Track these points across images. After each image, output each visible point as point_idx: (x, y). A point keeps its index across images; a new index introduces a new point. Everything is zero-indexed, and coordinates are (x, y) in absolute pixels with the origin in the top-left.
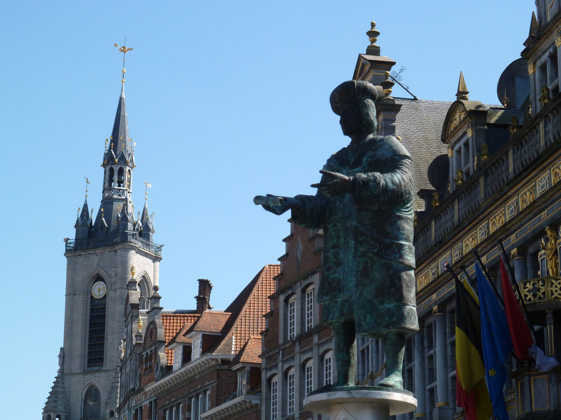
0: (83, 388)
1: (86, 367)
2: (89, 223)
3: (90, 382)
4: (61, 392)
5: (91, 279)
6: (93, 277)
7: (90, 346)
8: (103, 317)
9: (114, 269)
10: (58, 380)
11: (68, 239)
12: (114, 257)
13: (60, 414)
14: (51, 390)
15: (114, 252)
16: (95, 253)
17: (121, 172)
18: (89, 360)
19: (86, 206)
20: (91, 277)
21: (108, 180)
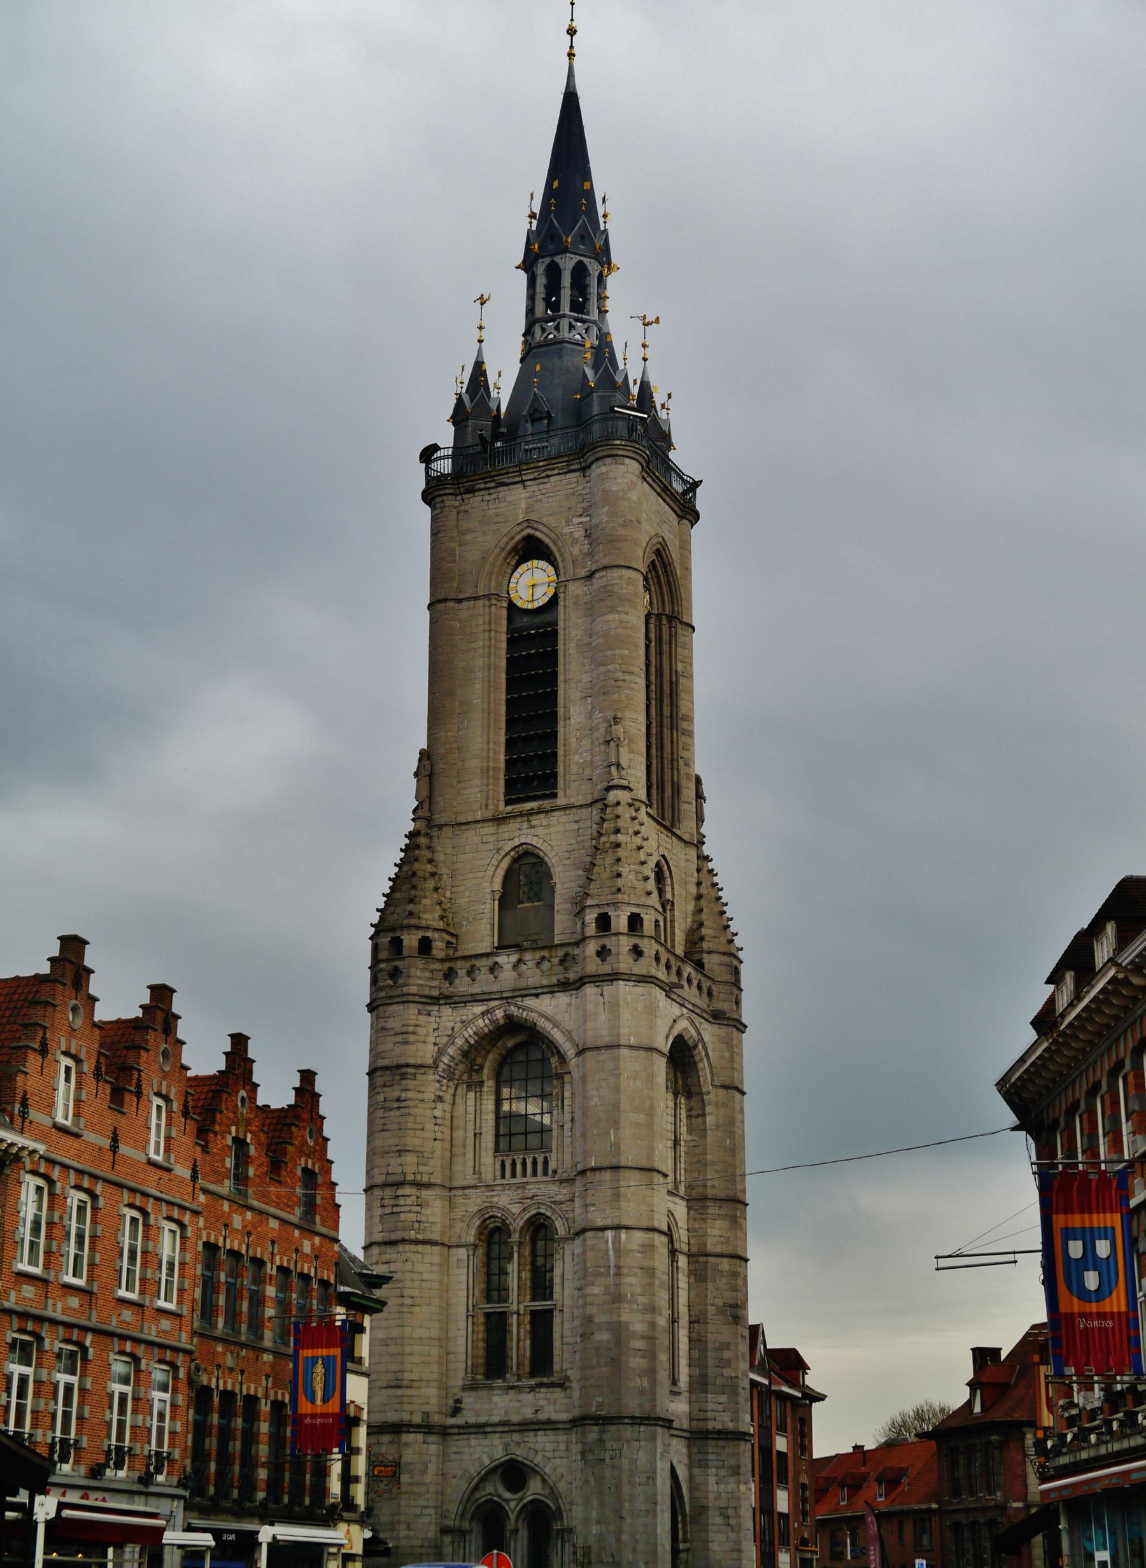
0: (494, 862)
1: (502, 803)
3: (517, 842)
4: (427, 875)
5: (509, 554)
6: (514, 549)
7: (510, 744)
9: (580, 520)
11: (434, 448)
12: (580, 488)
13: (429, 934)
15: (577, 474)
17: (580, 272)
18: (509, 784)
20: (509, 547)
21: (544, 296)
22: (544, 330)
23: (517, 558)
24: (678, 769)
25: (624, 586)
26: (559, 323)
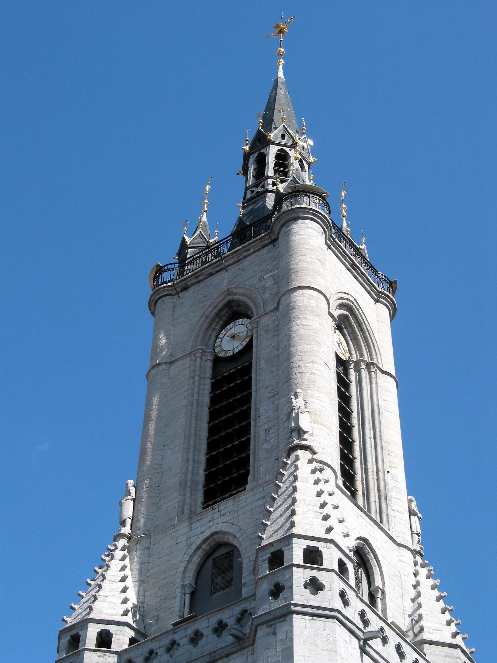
0: (187, 557)
5: (214, 319)
6: (218, 315)
9: (271, 274)
15: (269, 247)
20: (213, 315)
22: (252, 192)
23: (221, 323)
24: (385, 481)
25: (306, 300)
26: (264, 184)
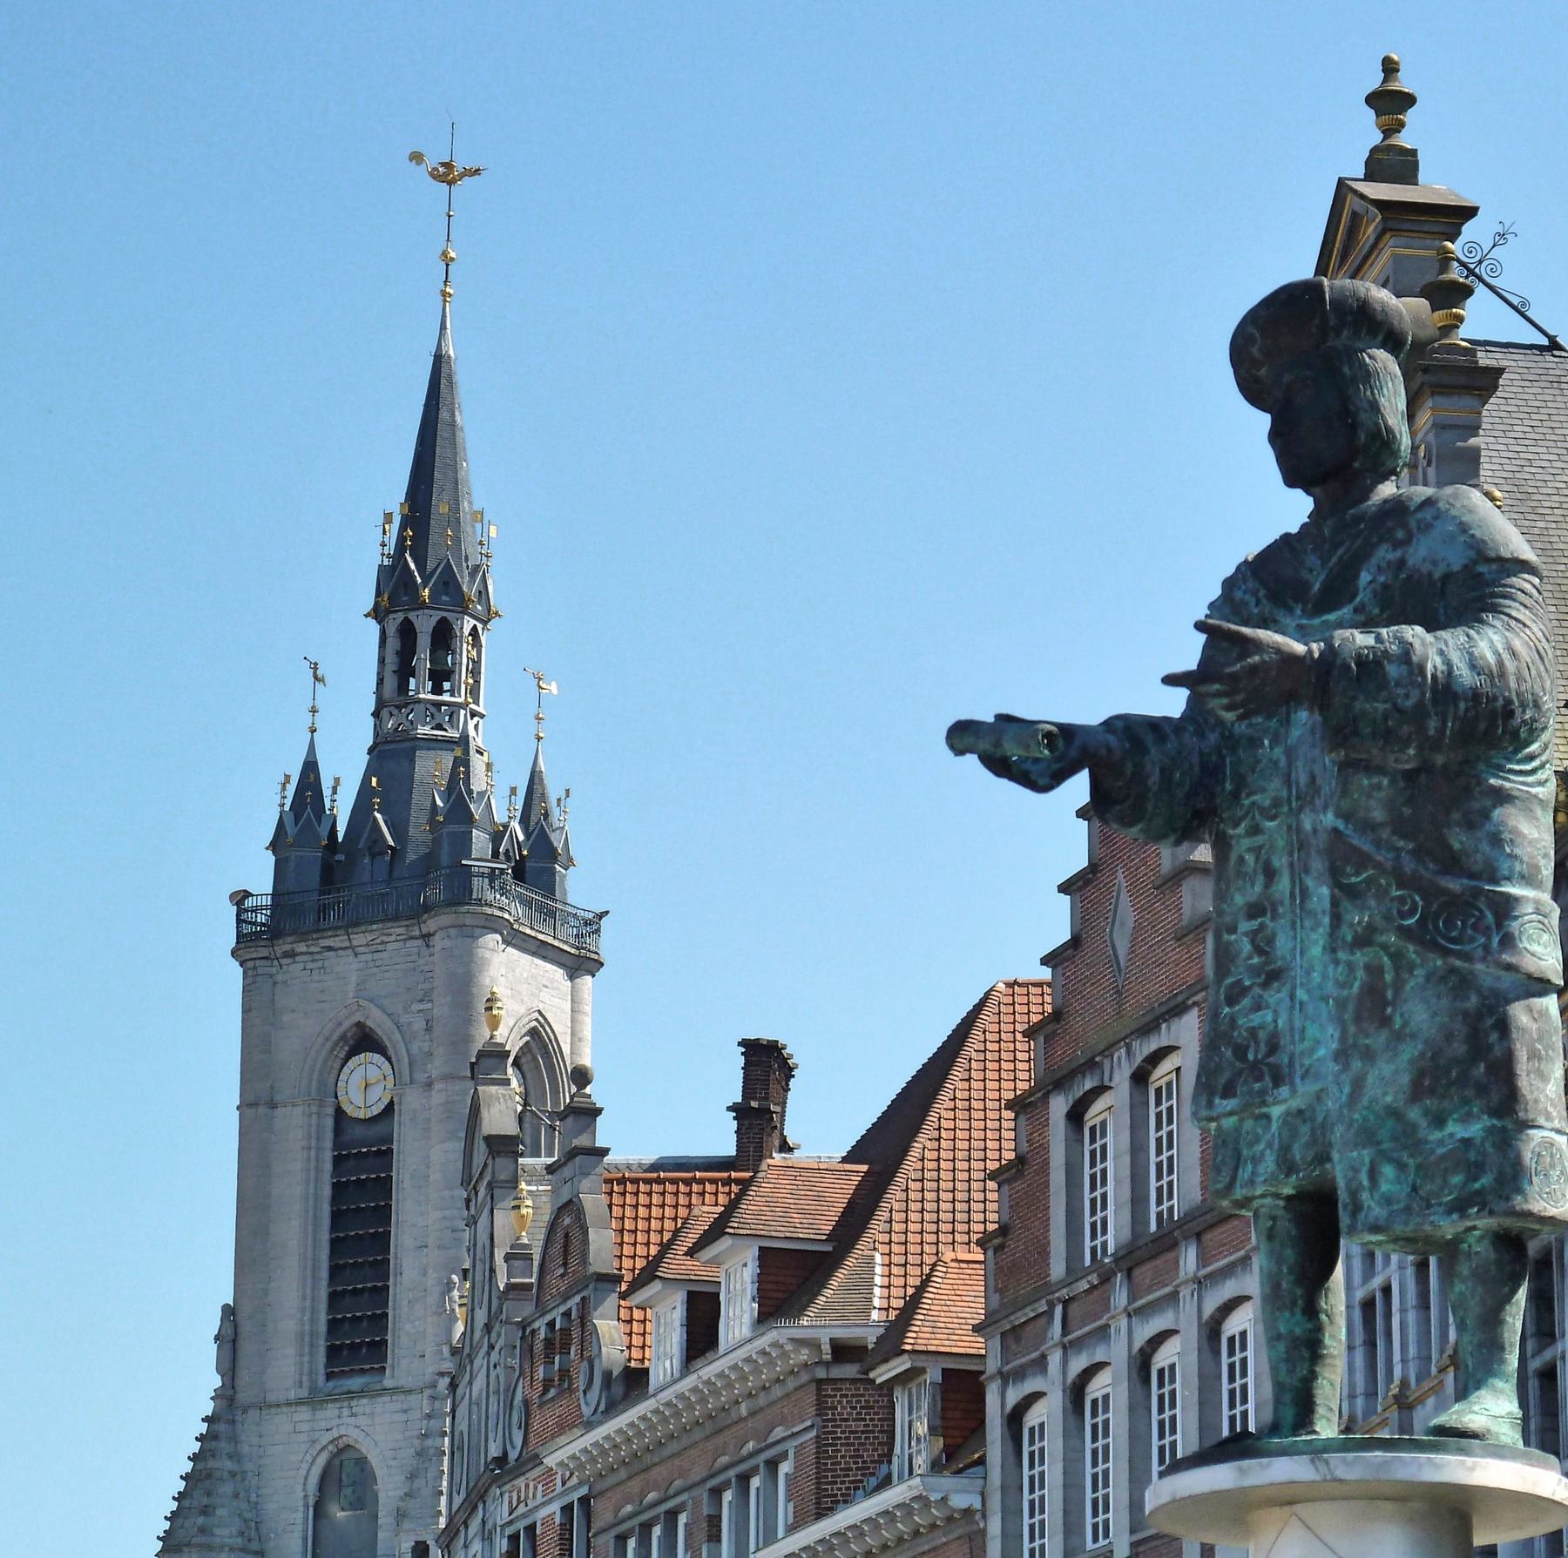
0: (309, 1458)
1: (321, 1378)
2: (324, 831)
4: (226, 1475)
5: (336, 1044)
6: (343, 1038)
8: (384, 1186)
10: (216, 1427)
11: (247, 894)
12: (421, 961)
14: (188, 1467)
15: (420, 942)
16: (347, 944)
17: (443, 637)
18: (333, 1352)
19: (310, 768)
20: (335, 1037)
23: (347, 1048)
